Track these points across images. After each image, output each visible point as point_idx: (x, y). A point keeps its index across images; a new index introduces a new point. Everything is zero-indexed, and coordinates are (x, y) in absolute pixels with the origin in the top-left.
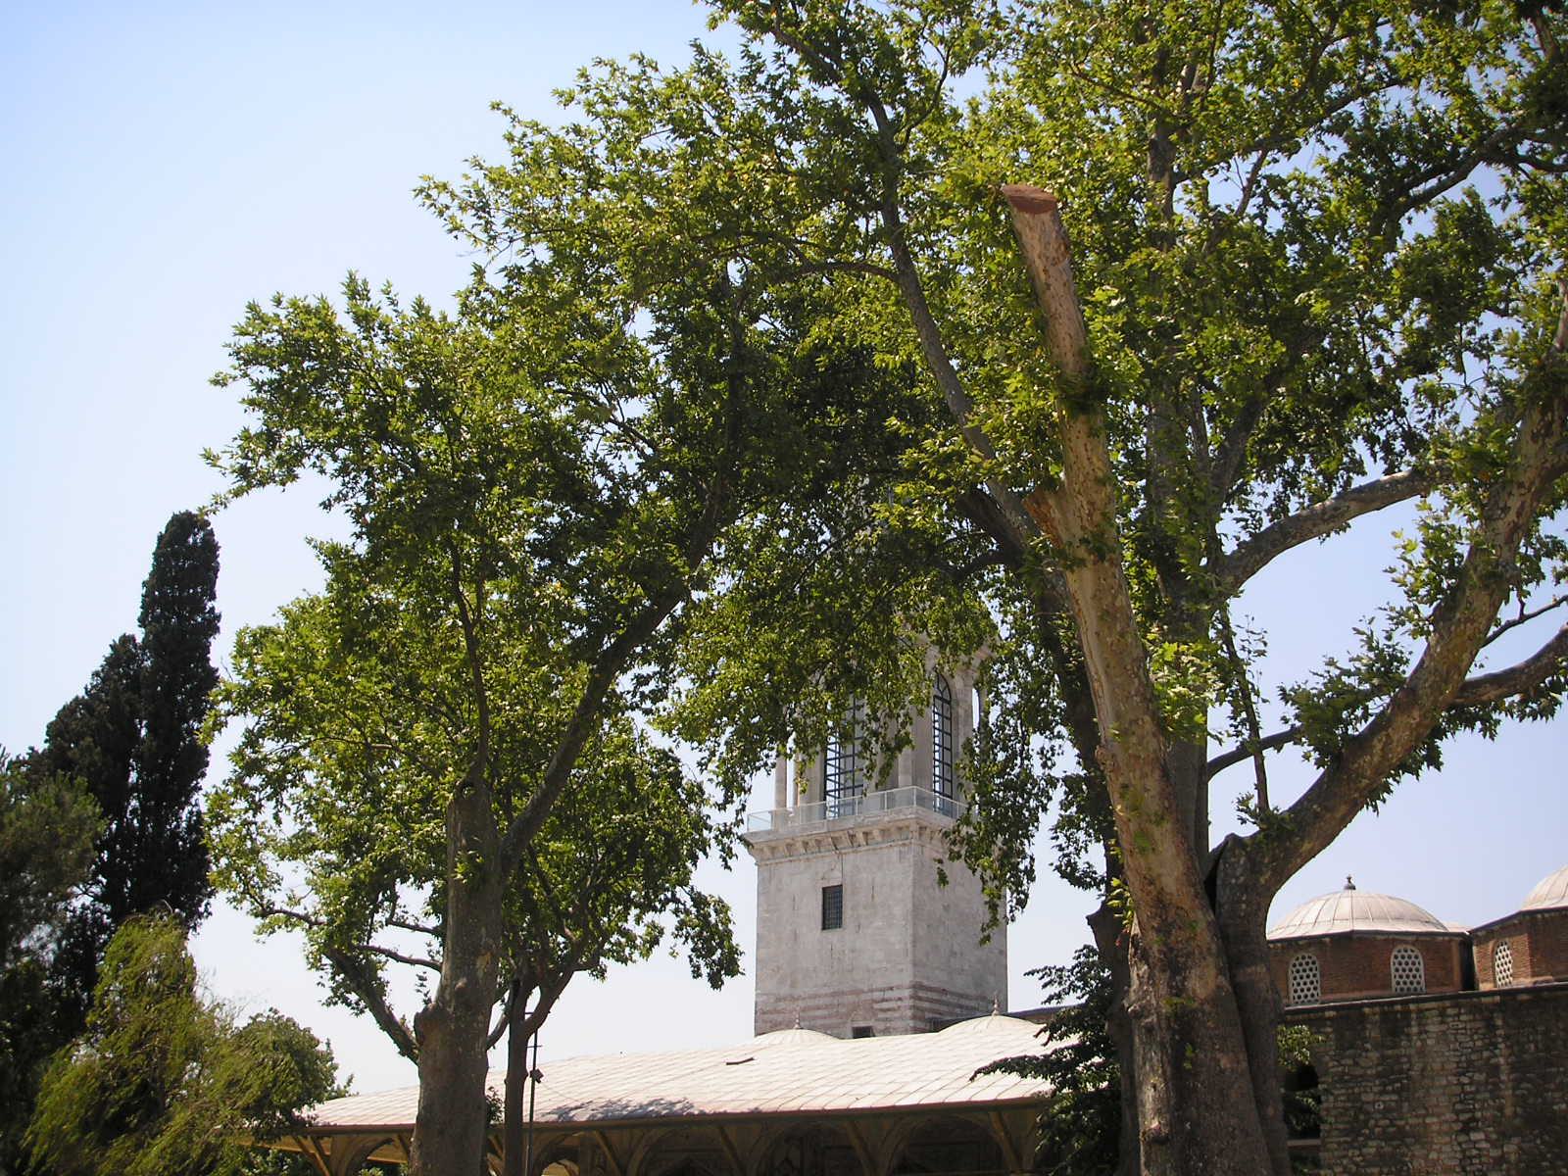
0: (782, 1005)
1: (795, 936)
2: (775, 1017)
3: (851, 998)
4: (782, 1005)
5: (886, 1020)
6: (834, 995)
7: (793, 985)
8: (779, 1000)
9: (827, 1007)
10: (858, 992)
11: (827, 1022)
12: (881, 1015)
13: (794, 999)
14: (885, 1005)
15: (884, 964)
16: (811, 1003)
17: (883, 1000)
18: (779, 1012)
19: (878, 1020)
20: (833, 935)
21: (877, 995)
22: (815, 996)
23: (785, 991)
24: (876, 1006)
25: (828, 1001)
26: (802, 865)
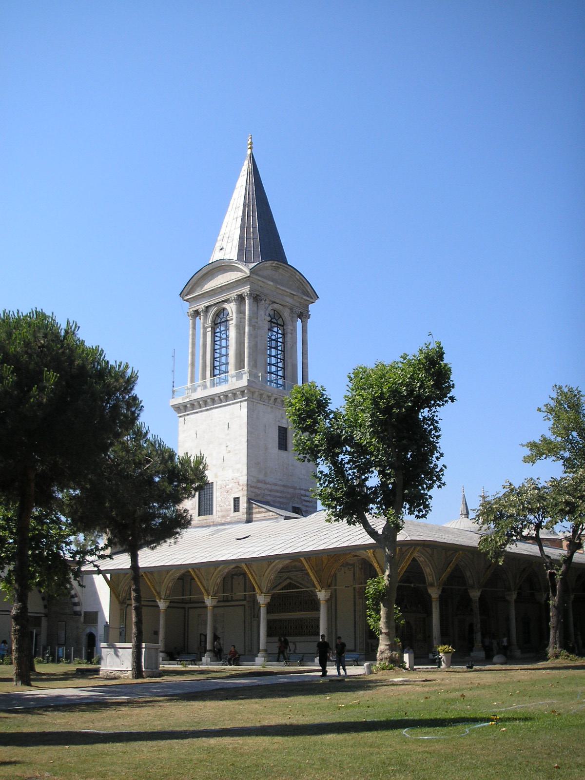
0: (260, 485)
1: (266, 449)
2: (256, 490)
3: (291, 490)
4: (260, 485)
5: (307, 506)
6: (284, 486)
7: (265, 475)
8: (258, 481)
9: (281, 492)
10: (295, 488)
11: (281, 500)
12: (304, 503)
13: (266, 483)
14: (306, 498)
15: (305, 477)
16: (274, 488)
17: (306, 496)
18: (258, 488)
19: (303, 505)
20: (283, 453)
21: (303, 492)
22: (276, 485)
23: (261, 477)
24: (303, 498)
25: (282, 488)
26: (269, 410)
